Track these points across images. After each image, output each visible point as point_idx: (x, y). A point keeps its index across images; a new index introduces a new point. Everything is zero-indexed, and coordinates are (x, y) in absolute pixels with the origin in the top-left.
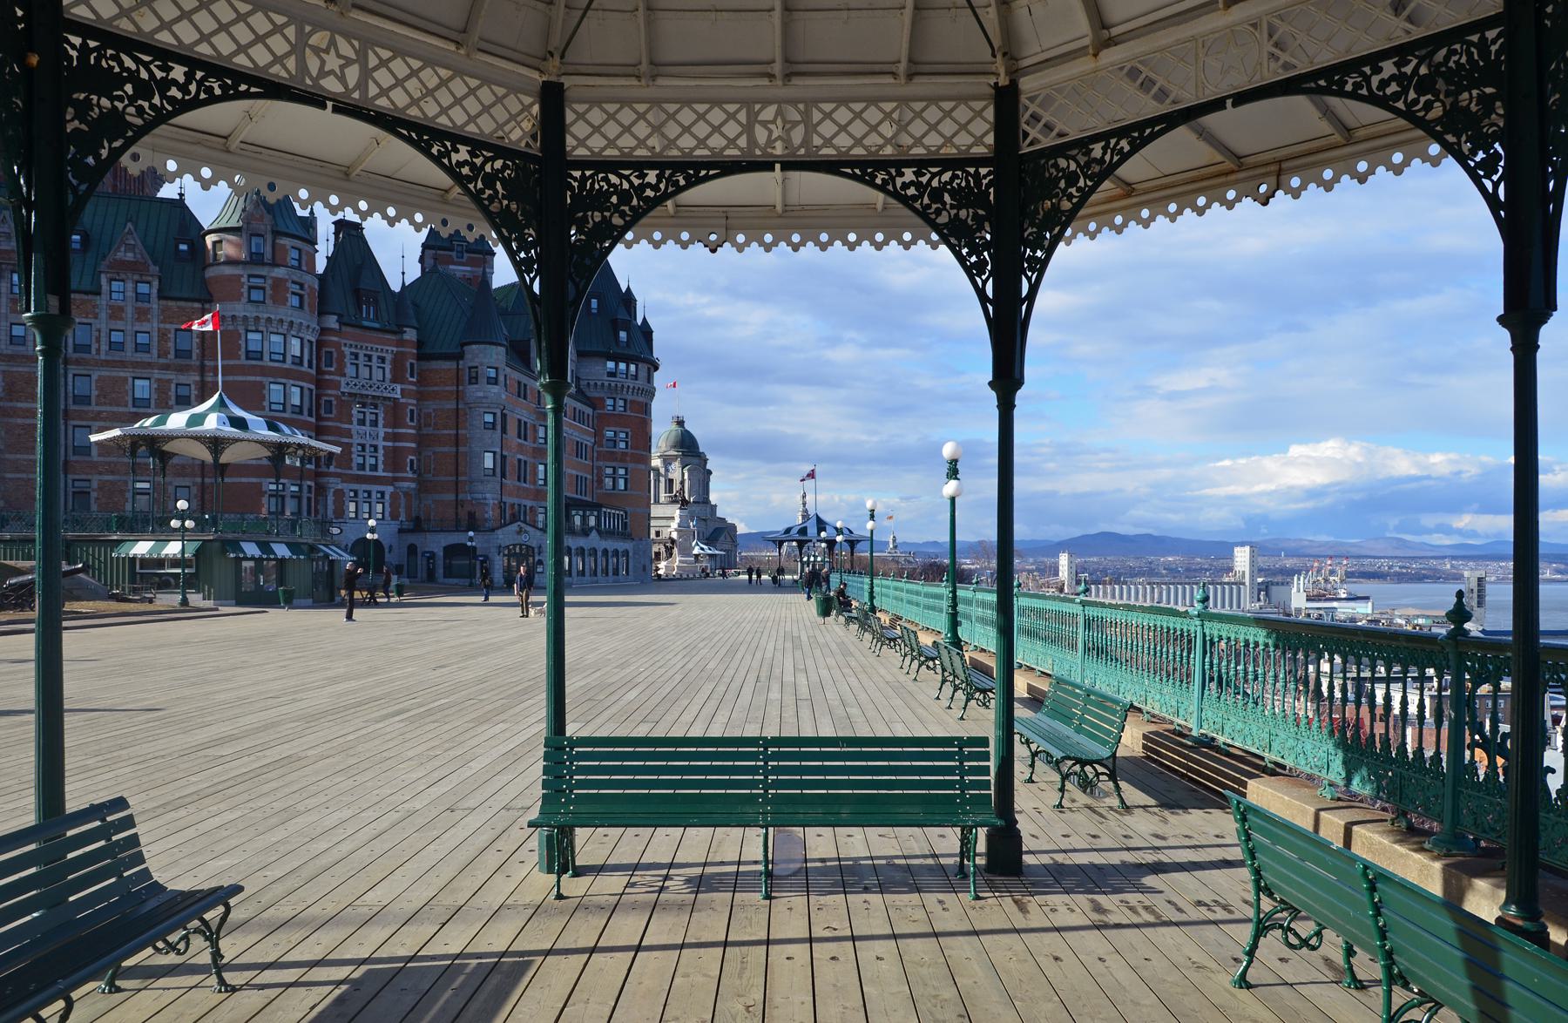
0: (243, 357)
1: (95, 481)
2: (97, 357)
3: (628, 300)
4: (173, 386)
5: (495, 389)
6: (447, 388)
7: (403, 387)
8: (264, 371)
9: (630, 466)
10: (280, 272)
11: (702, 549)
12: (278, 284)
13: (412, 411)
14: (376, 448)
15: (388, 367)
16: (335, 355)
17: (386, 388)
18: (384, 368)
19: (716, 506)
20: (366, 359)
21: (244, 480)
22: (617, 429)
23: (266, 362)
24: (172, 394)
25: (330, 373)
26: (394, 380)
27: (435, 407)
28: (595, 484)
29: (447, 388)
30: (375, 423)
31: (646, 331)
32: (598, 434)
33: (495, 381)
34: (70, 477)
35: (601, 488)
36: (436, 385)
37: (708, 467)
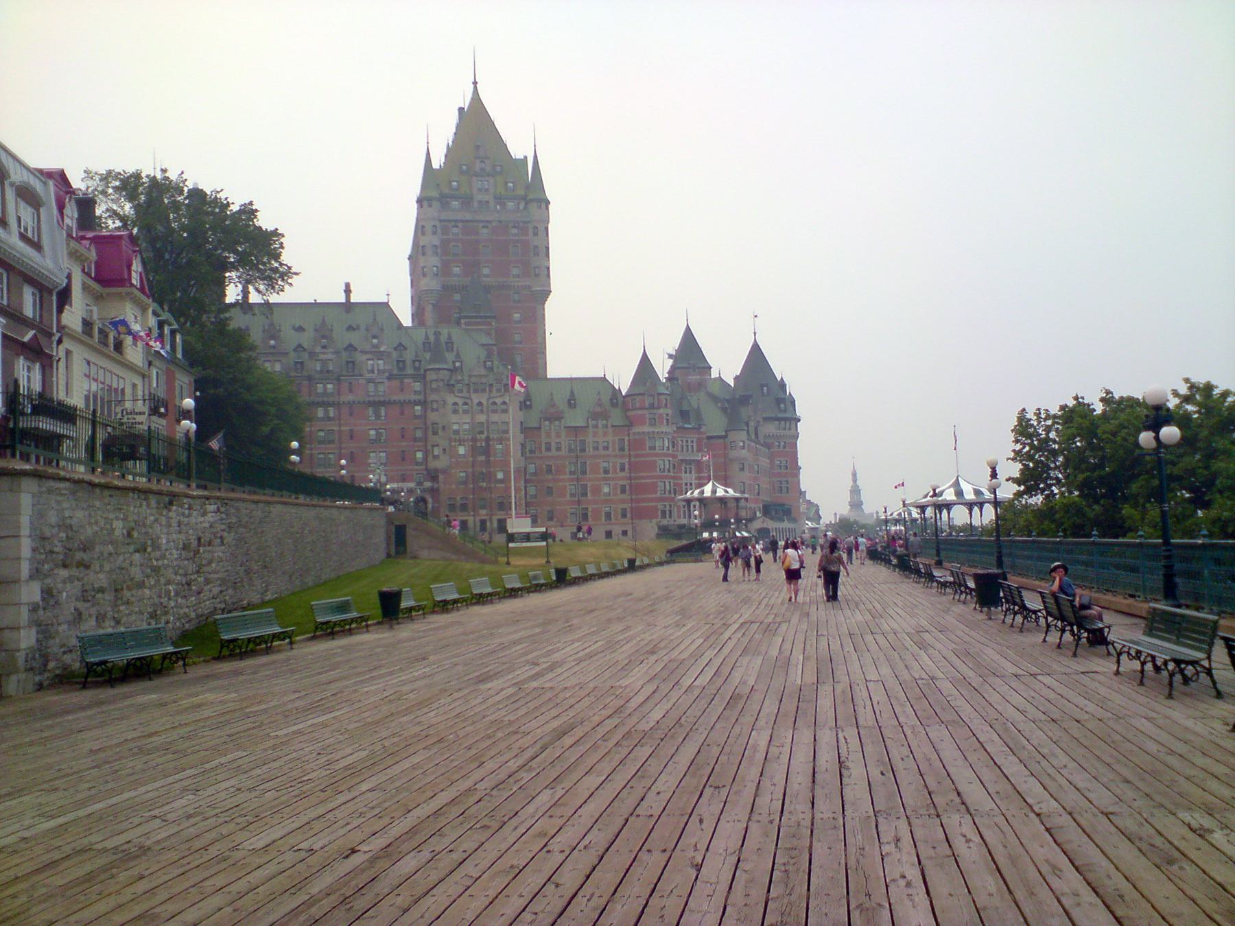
3: (782, 385)
5: (744, 452)
8: (656, 455)
10: (661, 411)
12: (661, 415)
14: (691, 484)
22: (782, 459)
23: (657, 451)
24: (618, 467)
26: (698, 451)
30: (690, 472)
31: (793, 403)
32: (772, 461)
33: (743, 448)
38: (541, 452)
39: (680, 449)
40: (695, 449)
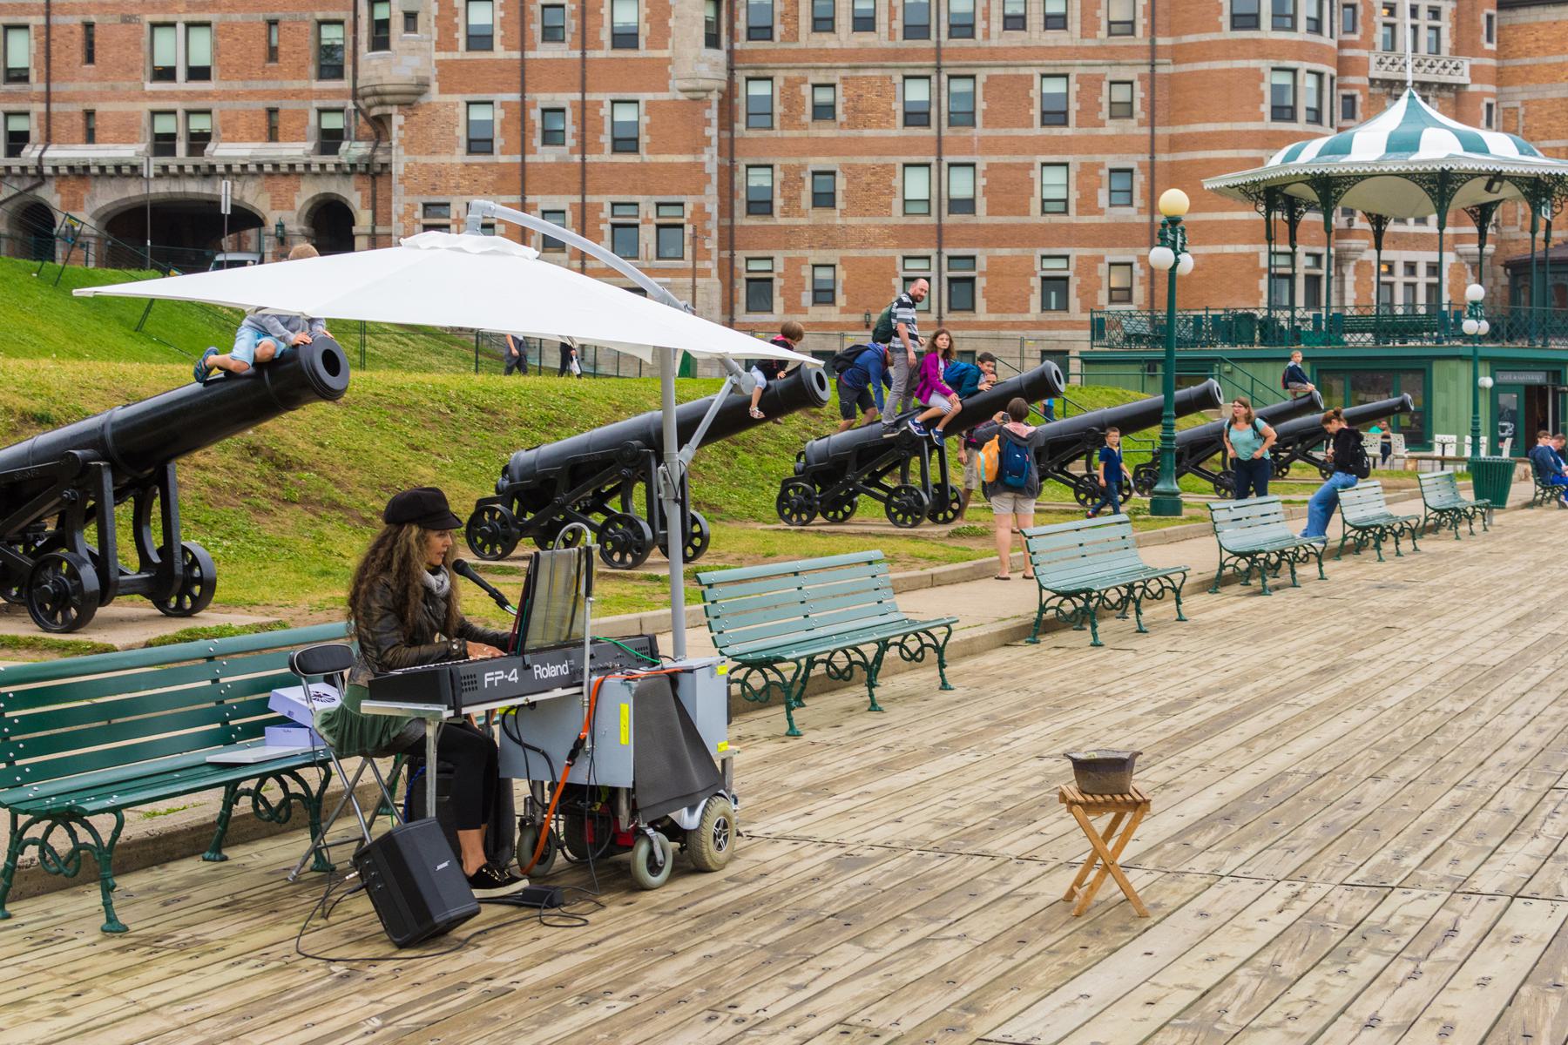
0: (1226, 24)
1: (982, 256)
2: (986, 44)
4: (1105, 86)
6: (1551, 59)
7: (1475, 61)
13: (1489, 106)
15: (1446, 25)
16: (1360, 10)
17: (1444, 67)
18: (1437, 29)
20: (1385, 12)
21: (1229, 249)
25: (1353, 45)
27: (1525, 97)
29: (1551, 59)
34: (947, 252)
36: (1528, 54)
38: (793, 35)
39: (1380, 34)
40: (1447, 42)
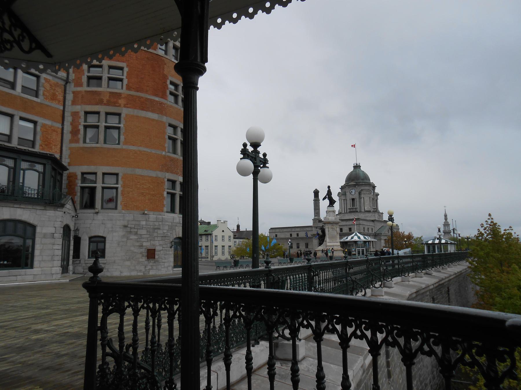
9: (125, 112)
11: (359, 238)
19: (382, 213)
28: (67, 136)
35: (77, 141)
37: (376, 191)
